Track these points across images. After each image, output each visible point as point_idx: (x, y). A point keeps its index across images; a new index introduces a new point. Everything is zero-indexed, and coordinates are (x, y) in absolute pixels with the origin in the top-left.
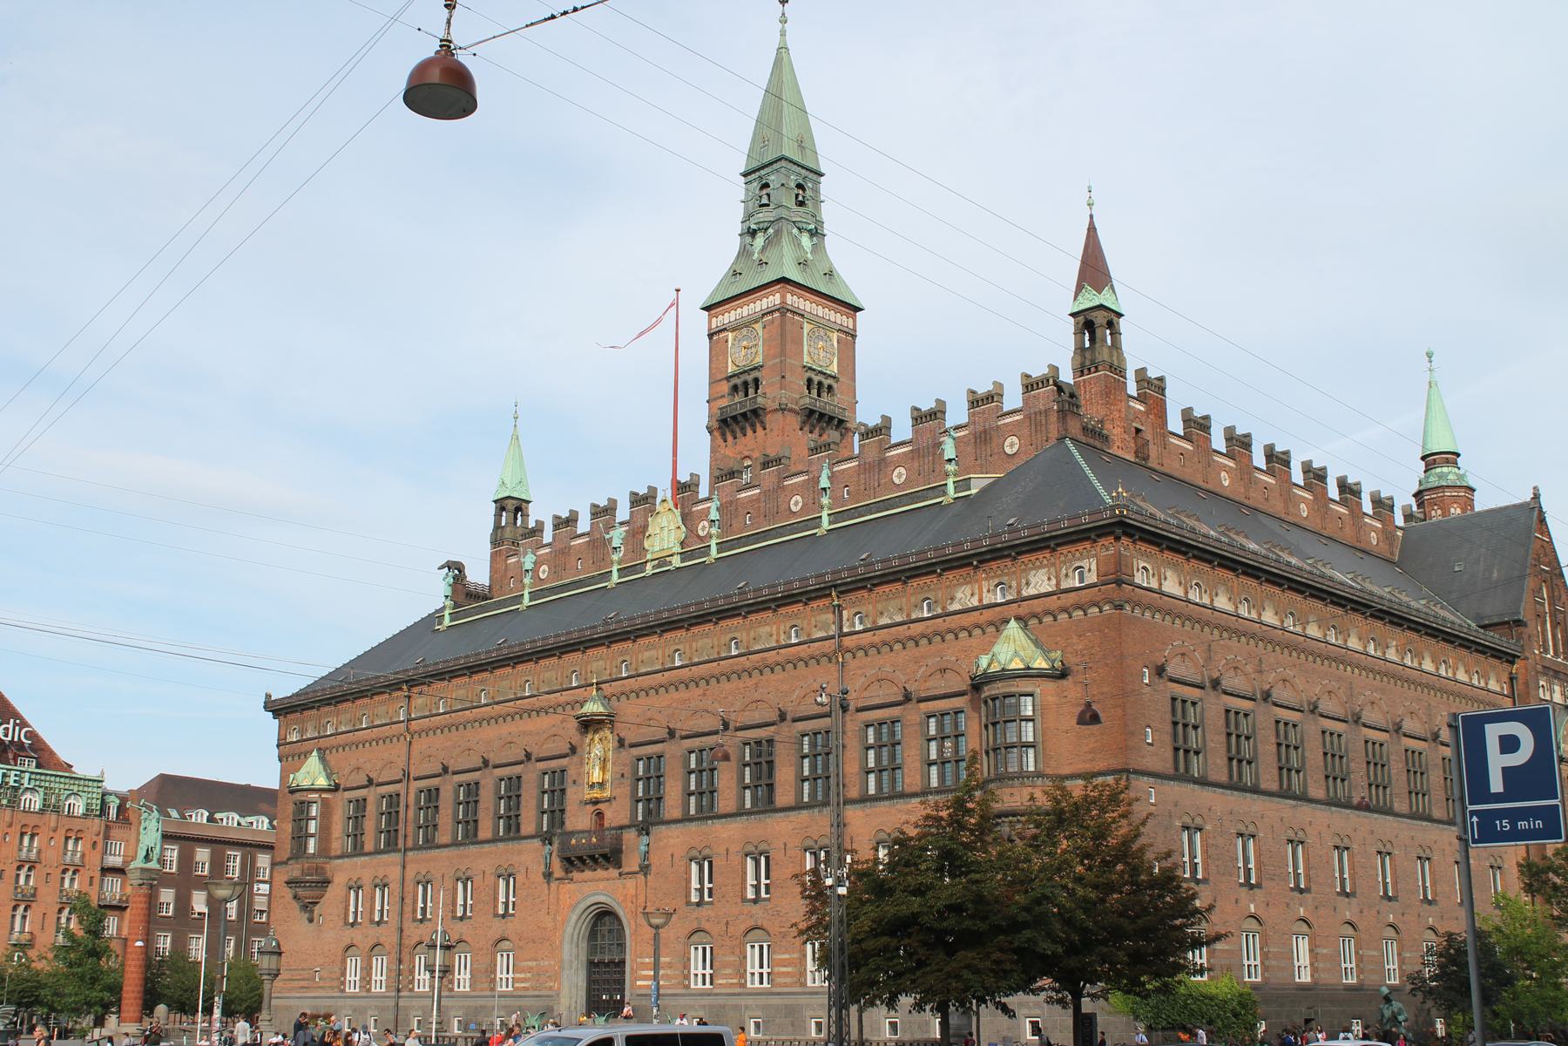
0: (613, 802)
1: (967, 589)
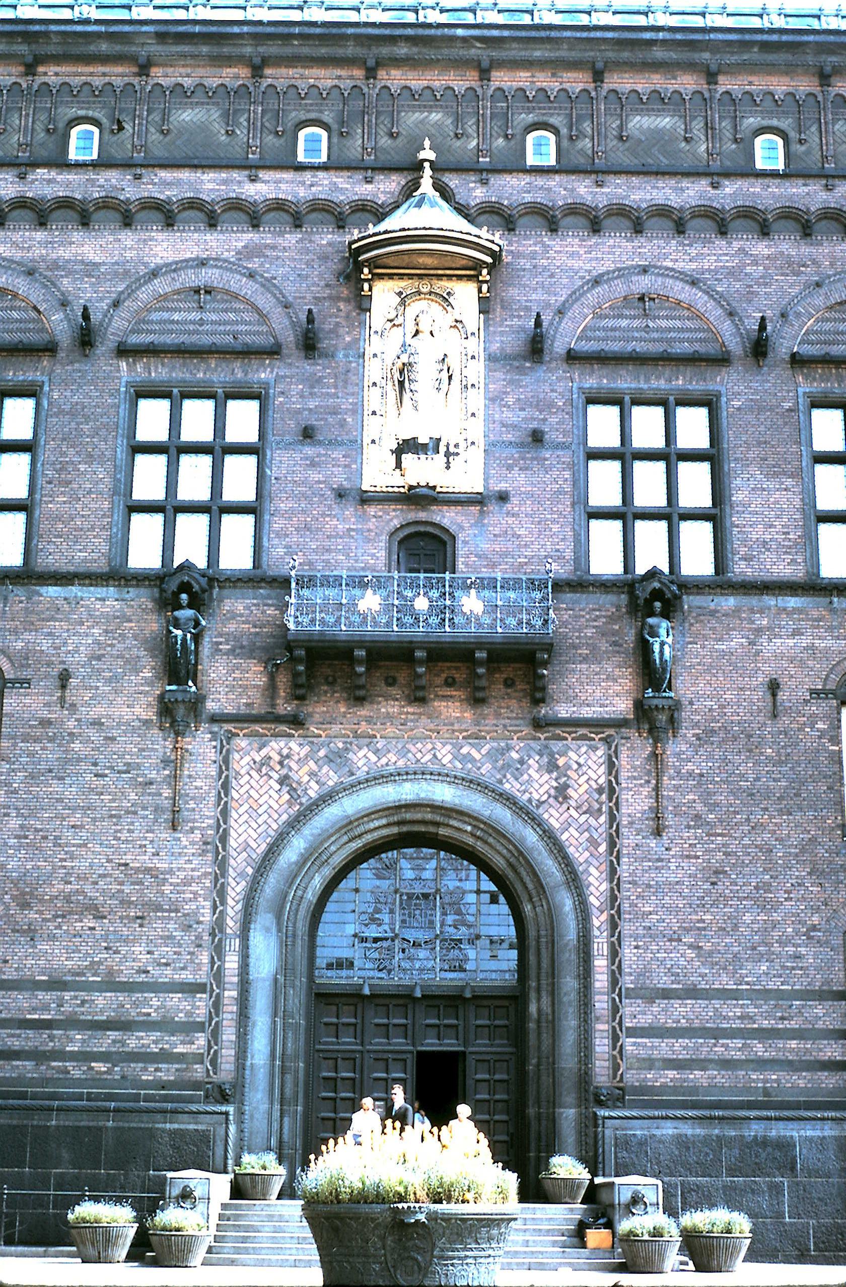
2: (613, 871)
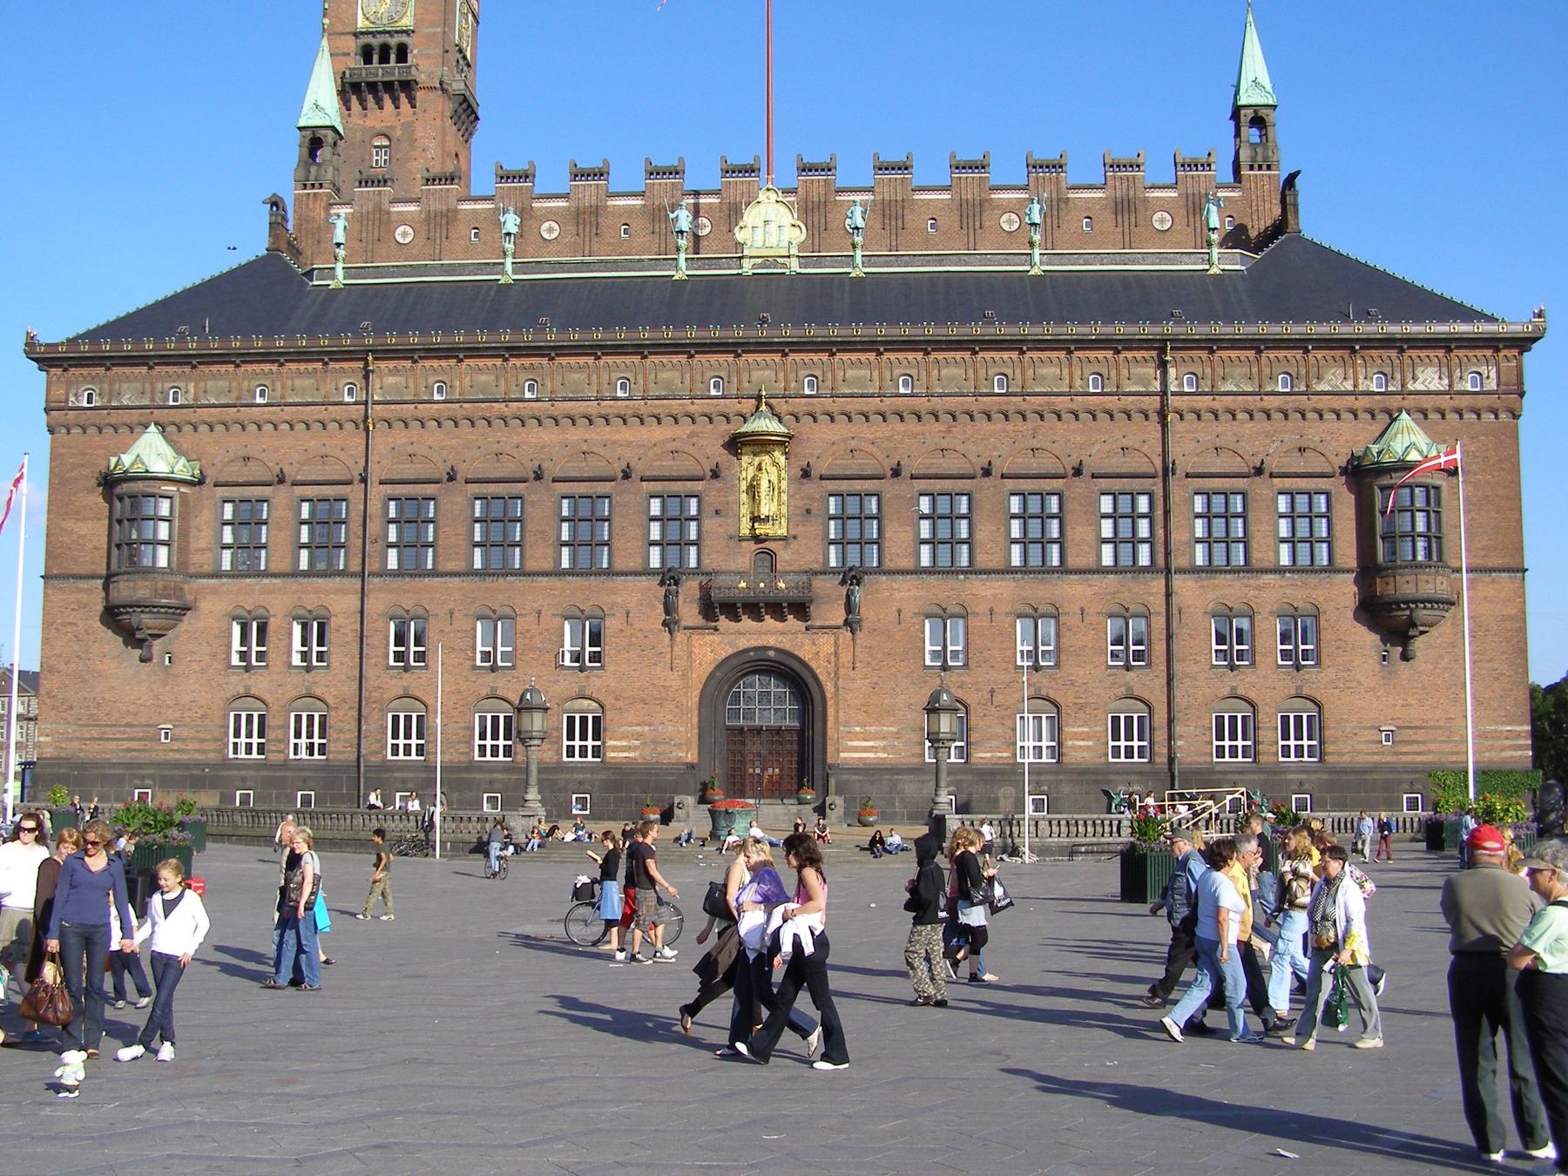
0: (794, 545)
1: (1340, 371)
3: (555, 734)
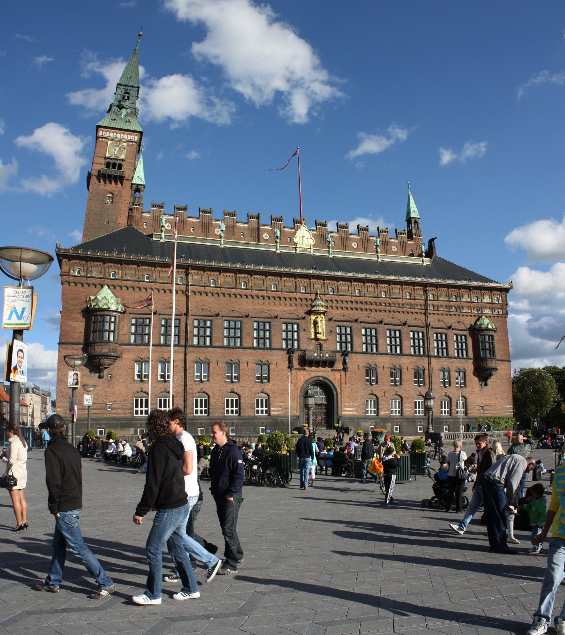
2: (341, 389)
3: (254, 405)
